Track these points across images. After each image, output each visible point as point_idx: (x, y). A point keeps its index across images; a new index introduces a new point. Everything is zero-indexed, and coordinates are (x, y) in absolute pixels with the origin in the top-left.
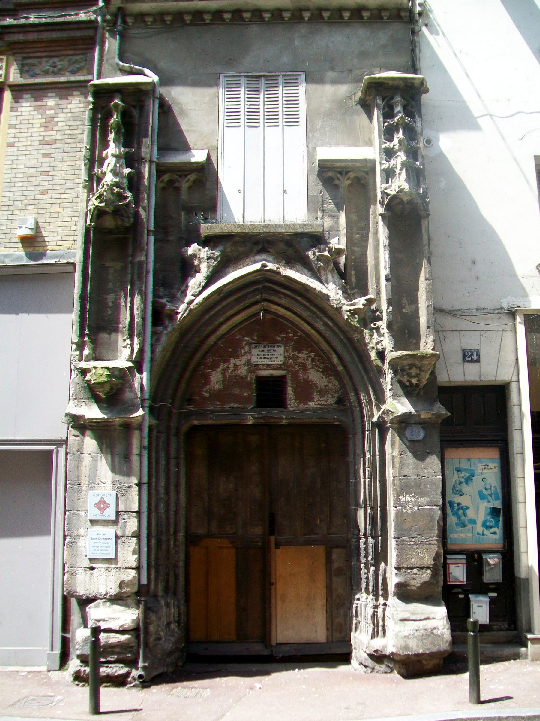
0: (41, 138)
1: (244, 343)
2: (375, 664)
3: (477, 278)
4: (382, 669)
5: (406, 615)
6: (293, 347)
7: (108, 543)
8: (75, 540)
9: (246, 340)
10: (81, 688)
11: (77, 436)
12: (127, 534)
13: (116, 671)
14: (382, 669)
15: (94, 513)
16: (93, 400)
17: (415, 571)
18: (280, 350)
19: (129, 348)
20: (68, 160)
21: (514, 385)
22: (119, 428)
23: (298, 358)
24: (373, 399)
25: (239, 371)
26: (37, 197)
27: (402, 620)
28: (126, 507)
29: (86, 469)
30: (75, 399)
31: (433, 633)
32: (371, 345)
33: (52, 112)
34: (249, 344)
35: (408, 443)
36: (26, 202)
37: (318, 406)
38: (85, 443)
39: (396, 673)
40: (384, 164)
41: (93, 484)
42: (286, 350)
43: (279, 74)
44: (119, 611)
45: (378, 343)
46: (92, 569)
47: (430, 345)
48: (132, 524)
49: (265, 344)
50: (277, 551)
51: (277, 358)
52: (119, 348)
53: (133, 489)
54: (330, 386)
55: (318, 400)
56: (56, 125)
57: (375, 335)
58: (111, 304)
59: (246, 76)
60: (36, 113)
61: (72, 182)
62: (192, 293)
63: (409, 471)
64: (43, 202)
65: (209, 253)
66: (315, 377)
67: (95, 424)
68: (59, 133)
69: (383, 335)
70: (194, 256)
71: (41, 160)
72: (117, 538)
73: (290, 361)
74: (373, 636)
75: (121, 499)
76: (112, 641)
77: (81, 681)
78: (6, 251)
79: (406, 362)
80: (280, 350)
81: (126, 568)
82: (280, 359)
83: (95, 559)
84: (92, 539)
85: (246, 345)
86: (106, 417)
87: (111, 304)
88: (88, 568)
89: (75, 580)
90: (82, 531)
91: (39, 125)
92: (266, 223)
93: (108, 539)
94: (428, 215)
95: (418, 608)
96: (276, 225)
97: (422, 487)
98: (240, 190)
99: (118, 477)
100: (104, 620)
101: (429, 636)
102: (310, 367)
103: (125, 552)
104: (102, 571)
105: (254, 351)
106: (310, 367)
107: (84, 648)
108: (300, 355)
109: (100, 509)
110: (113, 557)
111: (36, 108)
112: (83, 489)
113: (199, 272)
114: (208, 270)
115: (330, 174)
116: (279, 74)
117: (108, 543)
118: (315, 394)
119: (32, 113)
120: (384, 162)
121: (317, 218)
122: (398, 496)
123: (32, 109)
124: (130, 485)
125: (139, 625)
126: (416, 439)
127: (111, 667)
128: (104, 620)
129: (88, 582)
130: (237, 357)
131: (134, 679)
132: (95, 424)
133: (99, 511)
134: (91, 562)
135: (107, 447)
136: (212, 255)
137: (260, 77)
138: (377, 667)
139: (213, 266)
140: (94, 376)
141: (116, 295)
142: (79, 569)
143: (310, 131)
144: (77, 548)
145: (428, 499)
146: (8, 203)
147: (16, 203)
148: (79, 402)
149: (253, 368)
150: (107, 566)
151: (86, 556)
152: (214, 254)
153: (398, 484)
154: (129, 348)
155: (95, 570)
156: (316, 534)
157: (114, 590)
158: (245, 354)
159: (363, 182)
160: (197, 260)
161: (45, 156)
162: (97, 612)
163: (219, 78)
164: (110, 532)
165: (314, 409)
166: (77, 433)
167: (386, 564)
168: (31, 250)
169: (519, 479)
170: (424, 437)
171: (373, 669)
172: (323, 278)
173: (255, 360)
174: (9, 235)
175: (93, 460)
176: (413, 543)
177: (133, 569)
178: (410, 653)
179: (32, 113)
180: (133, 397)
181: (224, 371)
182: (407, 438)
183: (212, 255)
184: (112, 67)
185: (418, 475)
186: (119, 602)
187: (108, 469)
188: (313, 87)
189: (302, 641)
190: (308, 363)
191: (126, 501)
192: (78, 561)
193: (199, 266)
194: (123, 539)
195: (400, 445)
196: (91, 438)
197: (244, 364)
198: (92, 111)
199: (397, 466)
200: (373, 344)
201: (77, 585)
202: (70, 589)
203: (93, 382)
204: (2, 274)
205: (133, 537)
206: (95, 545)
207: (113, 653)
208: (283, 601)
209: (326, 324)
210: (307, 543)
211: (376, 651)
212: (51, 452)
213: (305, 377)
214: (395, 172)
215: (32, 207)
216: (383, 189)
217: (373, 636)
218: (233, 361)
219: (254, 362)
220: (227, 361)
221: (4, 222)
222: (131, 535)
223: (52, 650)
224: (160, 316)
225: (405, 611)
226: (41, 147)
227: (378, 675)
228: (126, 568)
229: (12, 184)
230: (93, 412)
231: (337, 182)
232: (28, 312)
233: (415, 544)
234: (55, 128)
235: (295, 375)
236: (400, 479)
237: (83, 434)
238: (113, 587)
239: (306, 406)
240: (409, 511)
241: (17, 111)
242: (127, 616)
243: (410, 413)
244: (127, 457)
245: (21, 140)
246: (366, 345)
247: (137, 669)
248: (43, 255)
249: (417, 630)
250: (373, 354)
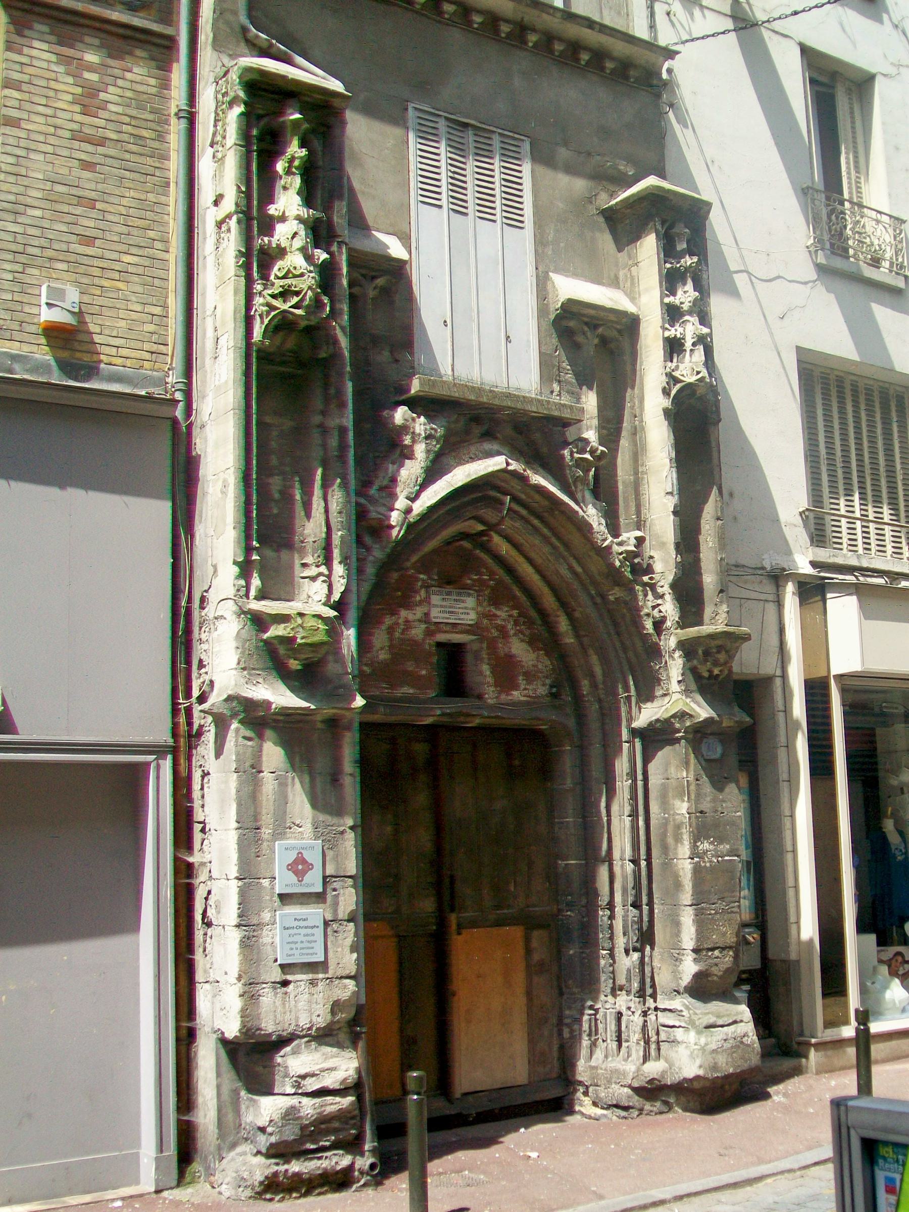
0: (75, 127)
1: (420, 584)
2: (645, 1102)
3: (735, 518)
4: (655, 1109)
5: (712, 1020)
6: (489, 597)
7: (313, 935)
8: (255, 934)
9: (423, 580)
10: (278, 1205)
11: (249, 739)
12: (340, 916)
13: (337, 1163)
14: (655, 1109)
15: (285, 882)
16: (275, 673)
17: (717, 953)
18: (471, 602)
19: (324, 581)
20: (131, 186)
21: (778, 682)
22: (319, 725)
23: (495, 615)
24: (633, 692)
25: (413, 632)
26: (73, 247)
27: (707, 1027)
28: (337, 869)
29: (268, 800)
30: (244, 669)
31: (742, 1042)
32: (646, 611)
33: (94, 77)
34: (427, 587)
35: (703, 763)
36: (50, 253)
37: (525, 699)
38: (264, 752)
39: (680, 1111)
40: (667, 329)
41: (282, 829)
42: (479, 603)
43: (495, 129)
44: (332, 1057)
45: (654, 607)
46: (285, 983)
47: (722, 617)
48: (348, 899)
49: (449, 588)
50: (459, 937)
51: (468, 614)
52: (296, 579)
53: (347, 836)
54: (540, 667)
55: (525, 689)
56: (102, 106)
57: (650, 597)
58: (277, 496)
59: (447, 119)
60: (61, 69)
61: (141, 232)
62: (405, 493)
63: (706, 805)
64: (85, 260)
65: (428, 427)
66: (519, 648)
67: (281, 718)
68: (111, 126)
69: (662, 596)
70: (404, 429)
71: (77, 172)
72: (326, 924)
73: (485, 621)
74: (646, 1058)
75: (330, 854)
76: (330, 1109)
77: (276, 1193)
78: (14, 348)
79: (714, 643)
80: (471, 602)
81: (342, 978)
82: (471, 618)
83: (290, 964)
84: (285, 928)
85: (422, 587)
86: (313, 707)
87: (277, 496)
88: (278, 983)
89: (258, 1007)
90: (266, 916)
91: (70, 98)
92: (511, 391)
93: (312, 927)
94: (720, 420)
95: (718, 1009)
96: (524, 397)
97: (721, 829)
98: (445, 322)
99: (322, 817)
100: (313, 1075)
101: (739, 1047)
102: (512, 632)
103: (339, 949)
104: (303, 988)
105: (435, 599)
106: (512, 632)
107: (284, 1129)
108: (498, 613)
109: (296, 873)
110: (322, 959)
111: (64, 60)
112: (265, 837)
113: (411, 459)
114: (427, 457)
115: (572, 324)
116: (495, 129)
117: (313, 935)
118: (521, 678)
119: (54, 67)
120: (667, 326)
121: (552, 392)
122: (695, 842)
123: (53, 58)
124: (341, 829)
125: (360, 1077)
126: (713, 757)
127: (326, 1157)
128: (313, 1075)
129: (280, 1009)
130: (408, 606)
131: (362, 1173)
132: (281, 718)
133: (296, 878)
134: (284, 973)
135: (302, 760)
136: (433, 432)
137: (466, 125)
138: (648, 1107)
139: (435, 452)
140: (301, 630)
141: (284, 480)
142: (264, 986)
143: (540, 242)
144: (259, 948)
145: (728, 847)
146: (14, 247)
147: (30, 250)
148: (250, 675)
149: (433, 628)
150: (310, 976)
151: (276, 960)
152: (436, 430)
153: (694, 824)
154: (324, 581)
155: (291, 986)
156: (509, 907)
157: (322, 1019)
158: (420, 603)
159: (612, 346)
160: (408, 437)
161: (87, 166)
162: (297, 1061)
163: (407, 109)
164: (315, 913)
165: (520, 703)
166: (249, 733)
167: (652, 949)
168: (65, 354)
169: (786, 818)
170: (723, 755)
171: (641, 1110)
172: (579, 496)
173: (437, 615)
174: (20, 316)
175: (280, 784)
176: (713, 912)
177: (349, 977)
178: (719, 1075)
179: (54, 67)
180: (340, 671)
181: (391, 630)
182: (703, 756)
183: (433, 432)
184: (231, 28)
185: (716, 811)
186: (327, 1039)
187: (306, 800)
188: (541, 169)
189: (495, 1087)
190: (509, 627)
191: (336, 858)
192: (262, 971)
193: (411, 448)
194: (335, 926)
195: (695, 765)
196: (275, 744)
197: (420, 621)
198: (244, 118)
199: (693, 797)
200: (647, 608)
201: (262, 1016)
202: (249, 1025)
203: (299, 641)
204: (2, 395)
205: (349, 921)
206: (291, 940)
207: (328, 1132)
208: (469, 1021)
209: (571, 568)
210: (499, 923)
211: (651, 1081)
212: (148, 764)
213: (506, 650)
214: (683, 345)
215: (63, 266)
216: (668, 370)
217: (646, 1058)
218: (404, 613)
219: (435, 617)
220: (394, 613)
221: (7, 285)
222: (346, 918)
223: (162, 1151)
224: (367, 526)
225: (708, 1013)
226: (76, 144)
227: (649, 1117)
228: (342, 978)
229: (21, 209)
230: (280, 696)
231: (580, 339)
232: (87, 485)
233: (715, 913)
234: (101, 113)
235: (492, 646)
236: (697, 817)
237: (261, 736)
238: (321, 1012)
239: (510, 698)
240: (708, 865)
241: (20, 53)
242: (343, 1065)
243: (712, 718)
244: (335, 779)
245: (34, 118)
246: (638, 609)
247: (362, 1154)
248: (92, 371)
249: (725, 1040)
250: (649, 625)
